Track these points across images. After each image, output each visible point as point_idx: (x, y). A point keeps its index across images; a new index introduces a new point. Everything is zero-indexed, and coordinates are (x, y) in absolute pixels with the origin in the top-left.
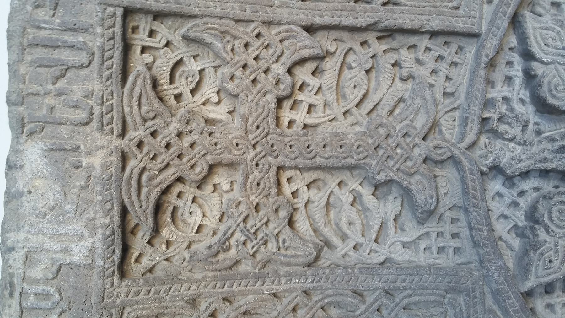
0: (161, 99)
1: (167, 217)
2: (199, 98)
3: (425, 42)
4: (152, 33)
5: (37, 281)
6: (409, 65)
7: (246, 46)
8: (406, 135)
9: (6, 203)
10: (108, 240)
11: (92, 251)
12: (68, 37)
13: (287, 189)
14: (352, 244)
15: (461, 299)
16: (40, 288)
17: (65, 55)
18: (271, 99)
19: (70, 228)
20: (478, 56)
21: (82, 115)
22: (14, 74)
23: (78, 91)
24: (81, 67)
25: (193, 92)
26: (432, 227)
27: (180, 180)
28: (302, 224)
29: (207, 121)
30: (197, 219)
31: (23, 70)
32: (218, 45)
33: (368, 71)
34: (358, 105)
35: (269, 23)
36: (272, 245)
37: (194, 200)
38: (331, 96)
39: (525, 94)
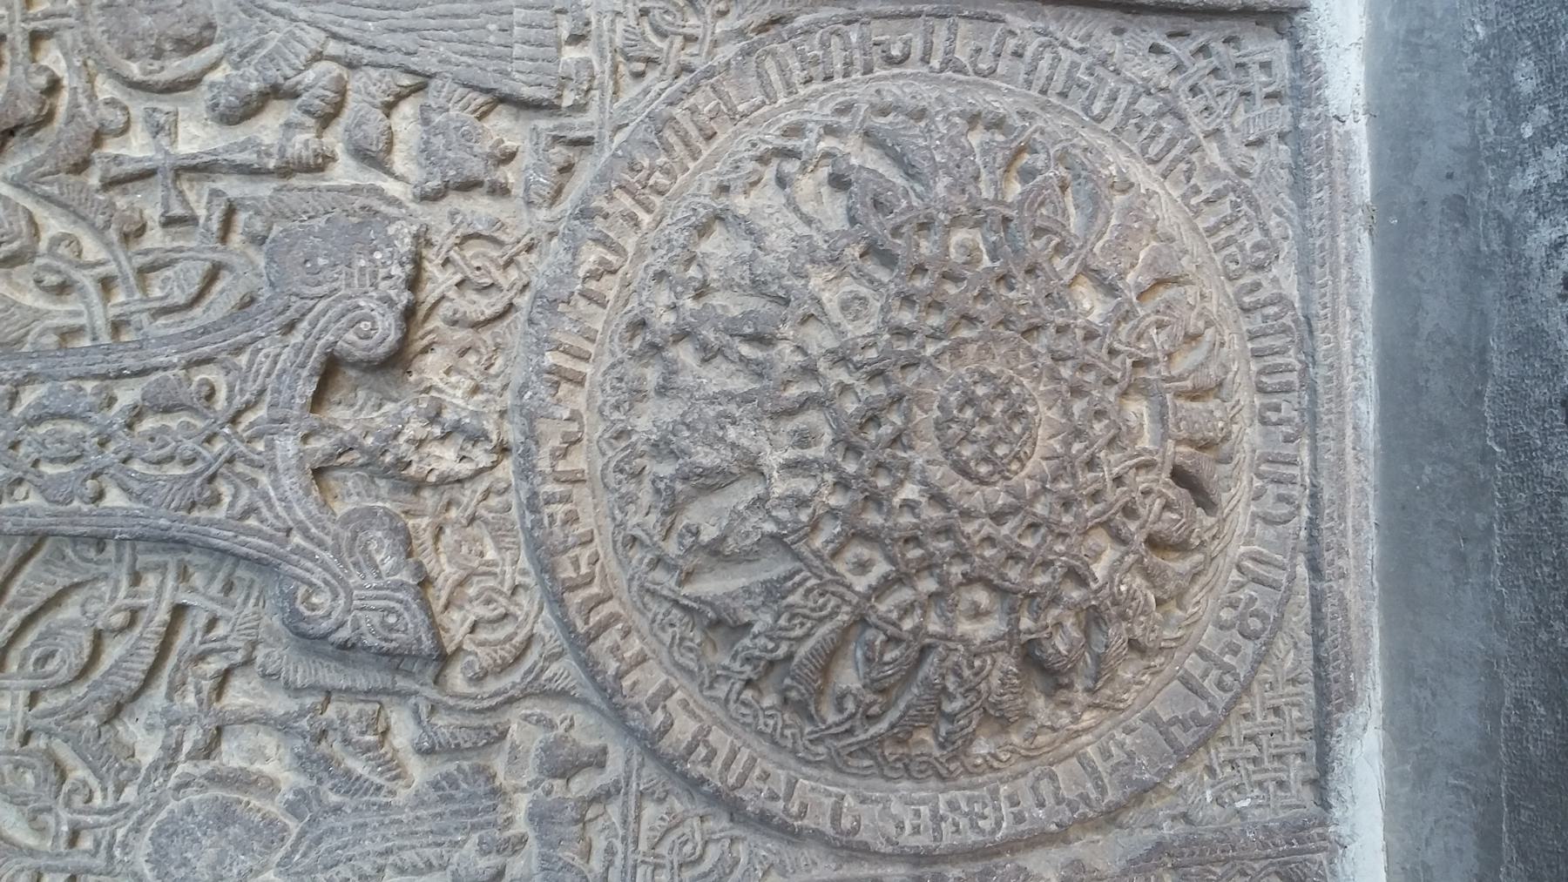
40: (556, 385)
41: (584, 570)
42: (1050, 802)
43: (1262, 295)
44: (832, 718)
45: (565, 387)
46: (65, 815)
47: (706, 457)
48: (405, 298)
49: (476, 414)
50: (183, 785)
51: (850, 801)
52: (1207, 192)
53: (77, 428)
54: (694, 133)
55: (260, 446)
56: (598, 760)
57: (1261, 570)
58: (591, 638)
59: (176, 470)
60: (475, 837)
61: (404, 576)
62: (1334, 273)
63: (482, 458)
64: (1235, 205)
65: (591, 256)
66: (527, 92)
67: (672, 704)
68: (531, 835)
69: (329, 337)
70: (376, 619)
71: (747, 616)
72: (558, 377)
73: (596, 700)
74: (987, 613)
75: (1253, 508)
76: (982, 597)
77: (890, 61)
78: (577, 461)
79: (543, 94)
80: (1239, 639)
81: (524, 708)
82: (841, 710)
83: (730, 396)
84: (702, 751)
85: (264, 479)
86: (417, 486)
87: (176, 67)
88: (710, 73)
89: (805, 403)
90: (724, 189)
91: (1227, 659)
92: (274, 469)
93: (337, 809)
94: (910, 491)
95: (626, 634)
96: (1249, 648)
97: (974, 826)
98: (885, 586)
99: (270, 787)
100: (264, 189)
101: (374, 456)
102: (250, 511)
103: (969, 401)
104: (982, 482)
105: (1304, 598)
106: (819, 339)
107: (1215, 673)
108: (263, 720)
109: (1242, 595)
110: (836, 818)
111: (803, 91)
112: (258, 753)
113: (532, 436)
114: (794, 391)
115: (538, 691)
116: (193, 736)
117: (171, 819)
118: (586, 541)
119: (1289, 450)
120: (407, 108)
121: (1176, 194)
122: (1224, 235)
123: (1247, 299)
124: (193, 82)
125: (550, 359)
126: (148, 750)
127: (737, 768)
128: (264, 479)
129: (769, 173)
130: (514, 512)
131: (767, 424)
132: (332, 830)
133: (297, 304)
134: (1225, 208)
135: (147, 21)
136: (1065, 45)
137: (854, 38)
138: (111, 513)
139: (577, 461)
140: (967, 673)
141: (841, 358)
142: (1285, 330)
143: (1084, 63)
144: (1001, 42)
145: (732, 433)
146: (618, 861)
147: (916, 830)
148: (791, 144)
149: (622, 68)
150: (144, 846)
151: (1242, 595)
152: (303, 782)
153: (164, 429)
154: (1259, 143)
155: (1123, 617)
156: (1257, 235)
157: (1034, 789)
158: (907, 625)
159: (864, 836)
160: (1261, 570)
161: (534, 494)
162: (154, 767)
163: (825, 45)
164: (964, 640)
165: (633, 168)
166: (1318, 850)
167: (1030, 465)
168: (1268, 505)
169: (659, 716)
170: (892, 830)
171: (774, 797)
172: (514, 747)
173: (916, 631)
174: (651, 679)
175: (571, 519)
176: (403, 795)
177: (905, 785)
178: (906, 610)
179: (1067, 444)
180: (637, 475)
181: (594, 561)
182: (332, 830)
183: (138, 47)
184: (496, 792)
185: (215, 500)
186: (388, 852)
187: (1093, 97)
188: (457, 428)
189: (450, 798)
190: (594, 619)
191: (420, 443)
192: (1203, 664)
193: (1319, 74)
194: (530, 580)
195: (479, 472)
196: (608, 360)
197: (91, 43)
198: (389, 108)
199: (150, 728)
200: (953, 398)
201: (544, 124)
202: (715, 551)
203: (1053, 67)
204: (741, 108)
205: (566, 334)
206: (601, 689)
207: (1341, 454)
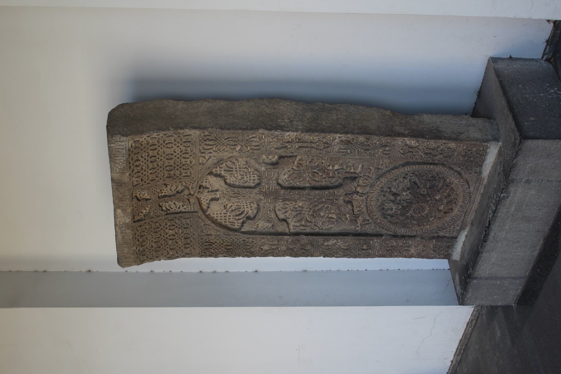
5: (121, 225)
11: (129, 221)
19: (125, 219)
34: (175, 190)
42: (421, 232)
51: (397, 229)
57: (457, 216)
58: (370, 214)
84: (380, 224)
91: (449, 223)
93: (340, 222)
96: (452, 223)
97: (410, 233)
99: (333, 218)
107: (447, 224)
127: (384, 225)
134: (464, 183)
145: (390, 204)
147: (403, 233)
150: (321, 223)
160: (457, 216)
168: (460, 210)
170: (401, 232)
171: (388, 228)
192: (446, 223)
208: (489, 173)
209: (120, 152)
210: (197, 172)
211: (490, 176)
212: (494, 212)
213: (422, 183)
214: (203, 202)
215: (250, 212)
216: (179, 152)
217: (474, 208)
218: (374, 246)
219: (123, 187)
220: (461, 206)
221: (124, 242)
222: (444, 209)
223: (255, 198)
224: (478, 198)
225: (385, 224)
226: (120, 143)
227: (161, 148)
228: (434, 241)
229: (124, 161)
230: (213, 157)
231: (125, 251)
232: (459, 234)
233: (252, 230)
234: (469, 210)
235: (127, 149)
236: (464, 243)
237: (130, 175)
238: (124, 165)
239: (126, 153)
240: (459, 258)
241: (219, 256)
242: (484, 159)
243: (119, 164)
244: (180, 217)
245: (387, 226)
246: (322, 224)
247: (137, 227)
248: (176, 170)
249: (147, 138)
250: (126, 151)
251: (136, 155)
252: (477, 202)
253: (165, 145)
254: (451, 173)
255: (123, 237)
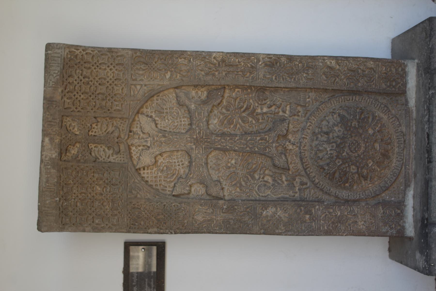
0: (67, 130)
1: (68, 151)
2: (74, 130)
3: (119, 119)
4: (66, 119)
5: (46, 161)
6: (115, 124)
7: (83, 121)
8: (113, 138)
9: (42, 148)
10: (59, 154)
11: (56, 156)
12: (53, 121)
13: (90, 147)
14: (103, 158)
15: (124, 169)
16: (47, 162)
17: (52, 123)
18: (87, 130)
19: (52, 152)
20: (128, 123)
21: (55, 133)
22: (43, 126)
23: (54, 130)
24: (55, 125)
25: (73, 129)
26: (119, 156)
27: (70, 145)
28: (93, 154)
29: (76, 135)
30: (73, 152)
31: (46, 126)
32: (78, 121)
33: (107, 125)
34: (105, 132)
35: (87, 117)
36: (87, 157)
37: (73, 149)
38: (99, 130)
39: (140, 130)
40: (304, 139)
41: (306, 161)
42: (364, 195)
43: (398, 131)
44: (335, 181)
45: (305, 139)
46: (249, 183)
47: (321, 148)
48: (287, 129)
49: (294, 142)
50: (261, 181)
51: (337, 192)
52: (391, 117)
53: (253, 142)
54: (322, 109)
55: (271, 145)
56: (306, 184)
57: (397, 168)
59: (262, 147)
60: (292, 191)
61: (286, 160)
62: (410, 128)
63: (294, 147)
64: (395, 119)
65: (309, 124)
66: (302, 104)
67: (316, 178)
68: (298, 192)
69: (279, 133)
70: (282, 165)
71: (325, 168)
72: (304, 138)
73: (307, 177)
74: (355, 169)
75: (396, 159)
76: (354, 167)
77: (347, 100)
78: (306, 148)
79: (304, 105)
80: (393, 177)
81: (298, 177)
82: (336, 180)
83: (324, 141)
84: (319, 184)
85: (271, 148)
86: (288, 149)
87: (264, 102)
88: (324, 102)
89: (333, 142)
90: (325, 117)
91: (391, 179)
92: (272, 147)
93: (277, 186)
94: (345, 154)
95: (310, 169)
96: (394, 178)
97: (353, 197)
98: (341, 164)
99: (269, 183)
100: (273, 116)
101: (283, 146)
102: (270, 151)
103: (352, 143)
104: (354, 153)
105: (404, 172)
106: (335, 135)
108: (269, 175)
109: (394, 171)
110: (335, 194)
111: (336, 104)
112: (268, 179)
113: (301, 145)
114: (332, 141)
115: (300, 175)
116: (262, 176)
117: (260, 185)
118: (306, 157)
119: (402, 152)
120: (288, 106)
121: (387, 117)
122: (393, 123)
123: (396, 131)
124: (265, 104)
125: (303, 136)
126: (257, 177)
128: (271, 148)
129: (331, 114)
130: (298, 154)
131: (328, 145)
132: (276, 188)
133: (276, 129)
134: (394, 119)
135: (261, 98)
136: (371, 98)
137: (343, 98)
138: (256, 151)
139: (306, 148)
140: (352, 177)
141: (338, 137)
142: (401, 136)
143: (374, 100)
144: (362, 98)
145: (324, 146)
146: (308, 196)
147: (346, 197)
148: (334, 111)
149: (314, 101)
150: (257, 187)
151: (394, 171)
152: (274, 183)
153: (262, 142)
154: (400, 110)
155: (374, 171)
156: (398, 123)
157: (362, 193)
158: (344, 170)
159: (339, 196)
160: (397, 168)
161: (300, 152)
162: (258, 179)
163: (339, 99)
164: (352, 172)
165: (314, 113)
166: (402, 206)
167: (360, 152)
168: (399, 159)
169: (314, 179)
170: (342, 196)
172: (297, 182)
173: (345, 171)
174: (313, 175)
175: (305, 155)
176: (284, 185)
177: (345, 191)
178: (344, 168)
179: (365, 149)
180: (313, 150)
181: (307, 160)
182: (276, 188)
183: (260, 100)
184: (294, 186)
185: (266, 150)
186: (282, 192)
187: (375, 105)
188: (292, 143)
189: (289, 186)
190: (307, 167)
191: (287, 145)
193: (408, 102)
194: (300, 162)
195: (294, 149)
196: (310, 136)
197: (256, 100)
198: (286, 106)
199: (257, 175)
200: (351, 143)
201: (304, 108)
202: (321, 159)
203: (369, 101)
204: (328, 106)
205: (305, 133)
206: (307, 175)
207: (410, 153)
208: (416, 102)
209: (56, 61)
210: (128, 106)
211: (418, 100)
212: (429, 121)
213: (351, 115)
214: (133, 155)
215: (182, 171)
216: (111, 77)
217: (412, 155)
218: (317, 215)
219: (54, 106)
220: (398, 153)
221: (47, 188)
222: (380, 149)
223: (186, 147)
224: (413, 138)
225: (324, 185)
226: (57, 51)
227: (95, 68)
228: (381, 208)
229: (58, 71)
230: (144, 85)
231: (47, 202)
232: (405, 194)
233: (184, 192)
234: (407, 158)
235: (63, 58)
236: (413, 207)
237: (62, 91)
238: (58, 77)
239: (61, 62)
240: (414, 232)
241: (149, 231)
242: (406, 81)
243: (53, 75)
244: (109, 167)
245: (327, 188)
246: (258, 189)
247: (63, 168)
248: (107, 100)
249: (82, 52)
250: (61, 59)
251: (71, 69)
252: (413, 144)
253: (99, 65)
254: (378, 105)
255: (47, 181)
